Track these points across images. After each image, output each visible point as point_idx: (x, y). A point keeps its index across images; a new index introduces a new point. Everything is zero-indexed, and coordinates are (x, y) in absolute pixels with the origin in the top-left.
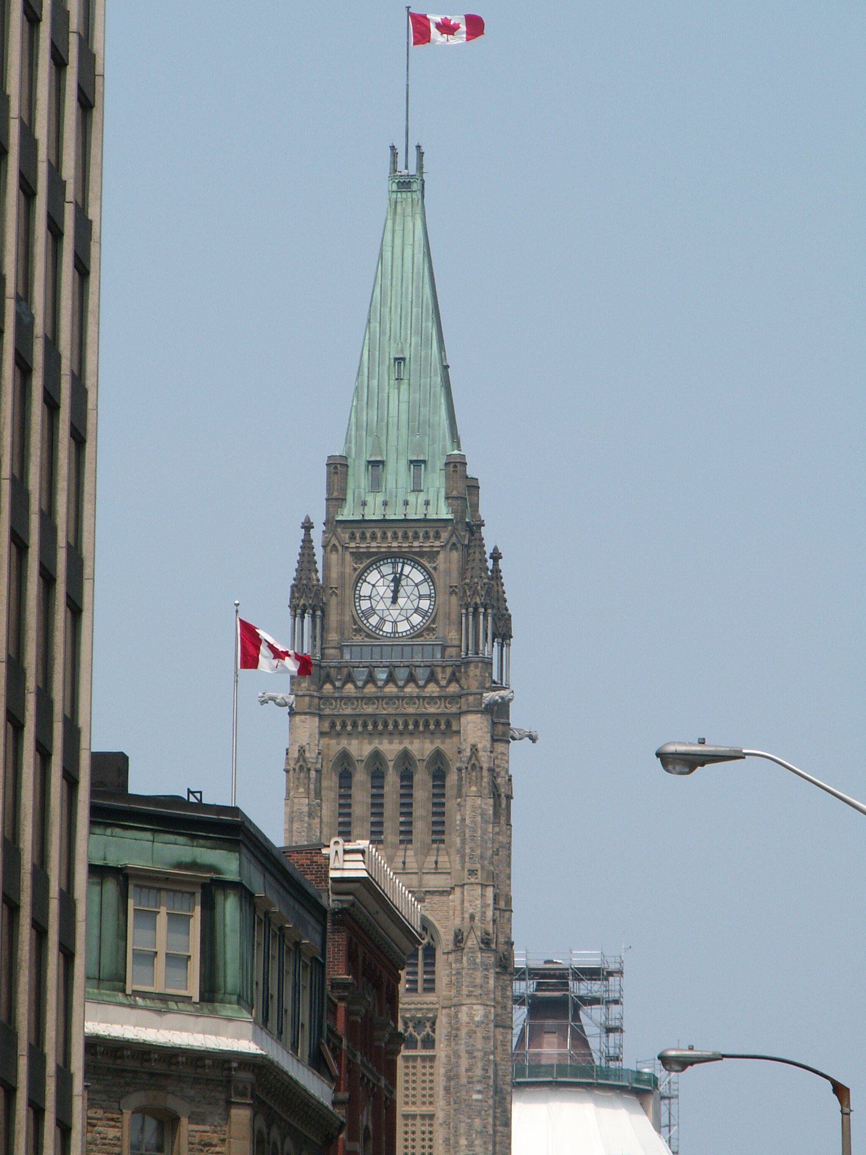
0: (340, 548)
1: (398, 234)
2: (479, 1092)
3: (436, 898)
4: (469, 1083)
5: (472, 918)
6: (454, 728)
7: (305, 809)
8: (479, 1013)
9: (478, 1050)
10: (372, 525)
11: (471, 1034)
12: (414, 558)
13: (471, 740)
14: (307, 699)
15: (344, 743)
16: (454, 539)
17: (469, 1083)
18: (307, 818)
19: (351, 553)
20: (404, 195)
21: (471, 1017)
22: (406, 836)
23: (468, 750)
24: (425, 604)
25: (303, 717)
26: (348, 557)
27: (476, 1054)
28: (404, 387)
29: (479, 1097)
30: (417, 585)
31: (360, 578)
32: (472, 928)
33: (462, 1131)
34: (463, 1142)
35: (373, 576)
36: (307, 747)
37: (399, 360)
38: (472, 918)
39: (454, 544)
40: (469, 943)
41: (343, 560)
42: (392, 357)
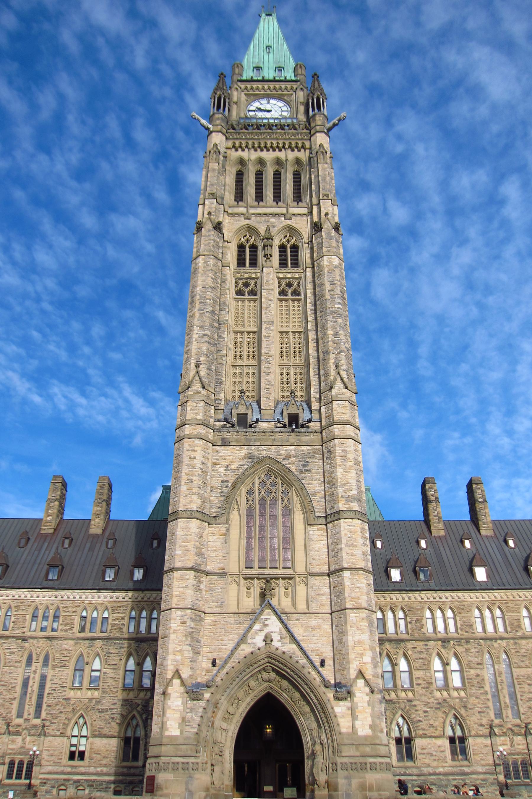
0: (239, 89)
1: (266, 26)
2: (339, 303)
3: (299, 218)
4: (331, 298)
5: (326, 214)
6: (307, 145)
7: (217, 168)
8: (336, 261)
9: (337, 280)
10: (257, 83)
11: (330, 272)
12: (280, 98)
13: (319, 143)
14: (220, 127)
15: (240, 153)
16: (301, 86)
17: (331, 298)
18: (217, 171)
19: (245, 94)
20: (268, 17)
21: (330, 262)
22: (278, 197)
23: (318, 146)
24: (285, 114)
25: (217, 133)
26: (243, 94)
27: (335, 282)
28: (271, 55)
29: (340, 306)
30: (280, 107)
31: (249, 104)
32: (328, 219)
33: (329, 325)
34: (330, 332)
35: (256, 104)
36: (219, 145)
37: (268, 47)
38: (326, 214)
39: (302, 89)
40: (326, 226)
41: (240, 94)
42: (265, 47)
